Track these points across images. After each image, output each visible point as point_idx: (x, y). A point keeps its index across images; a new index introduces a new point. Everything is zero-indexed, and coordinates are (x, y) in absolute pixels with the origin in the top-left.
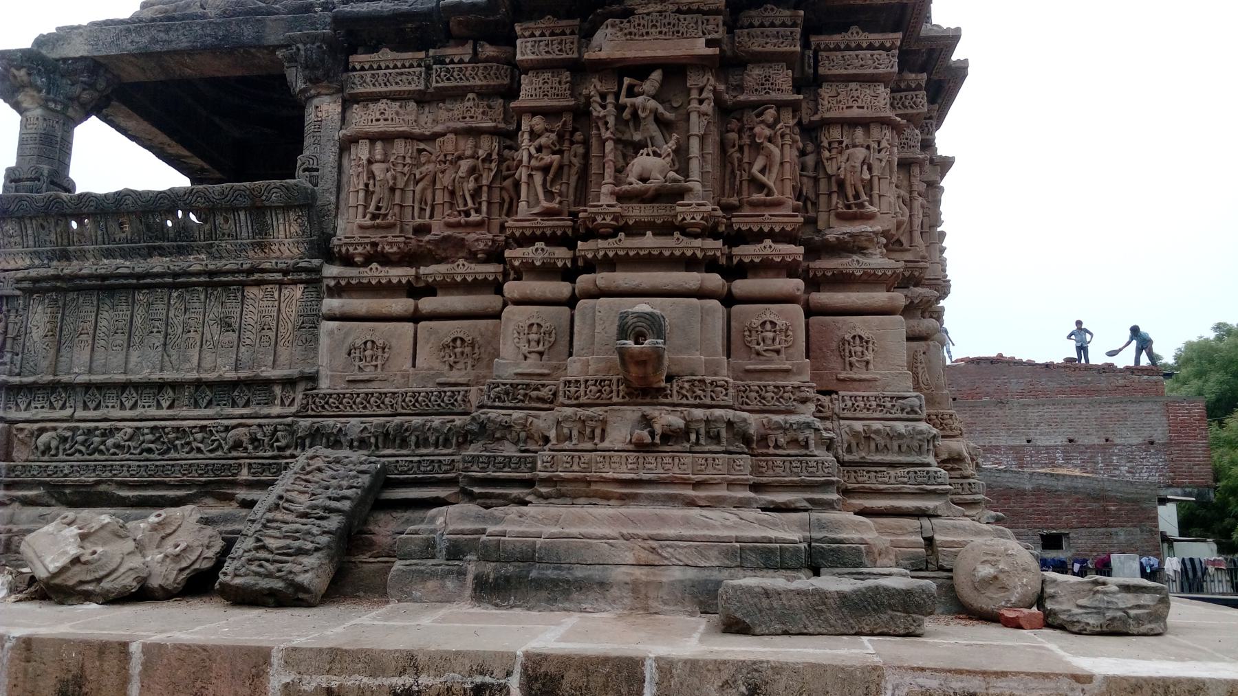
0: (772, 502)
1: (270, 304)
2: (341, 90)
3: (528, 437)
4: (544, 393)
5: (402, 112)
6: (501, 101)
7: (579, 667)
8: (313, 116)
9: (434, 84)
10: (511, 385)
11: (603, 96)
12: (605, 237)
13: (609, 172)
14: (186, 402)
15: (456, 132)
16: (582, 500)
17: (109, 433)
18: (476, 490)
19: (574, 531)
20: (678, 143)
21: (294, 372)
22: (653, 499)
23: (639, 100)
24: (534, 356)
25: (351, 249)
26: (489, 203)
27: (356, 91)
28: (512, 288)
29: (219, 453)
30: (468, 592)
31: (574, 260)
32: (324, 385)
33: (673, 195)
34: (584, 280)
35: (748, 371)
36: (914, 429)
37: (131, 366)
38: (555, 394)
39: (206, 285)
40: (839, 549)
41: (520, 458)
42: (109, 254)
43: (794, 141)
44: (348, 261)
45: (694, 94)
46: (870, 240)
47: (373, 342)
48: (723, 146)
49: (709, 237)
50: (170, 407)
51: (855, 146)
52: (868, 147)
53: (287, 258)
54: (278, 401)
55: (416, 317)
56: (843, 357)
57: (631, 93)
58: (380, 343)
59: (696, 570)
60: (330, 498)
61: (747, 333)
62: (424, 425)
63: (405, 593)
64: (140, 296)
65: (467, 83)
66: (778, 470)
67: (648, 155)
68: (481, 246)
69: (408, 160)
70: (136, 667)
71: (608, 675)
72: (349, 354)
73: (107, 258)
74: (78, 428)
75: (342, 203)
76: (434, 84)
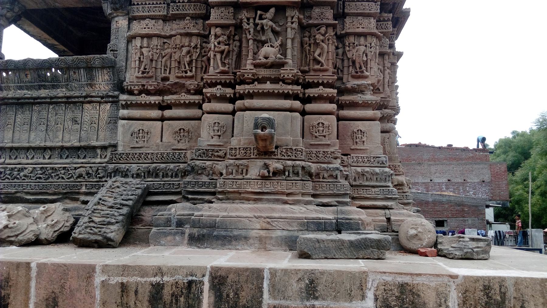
0: (321, 202)
1: (95, 112)
2: (128, 14)
3: (214, 173)
4: (221, 153)
5: (156, 25)
6: (202, 21)
7: (235, 273)
8: (115, 26)
9: (171, 12)
10: (206, 150)
11: (248, 19)
12: (248, 84)
13: (251, 54)
14: (57, 156)
15: (181, 35)
16: (237, 201)
17: (22, 170)
18: (190, 196)
19: (233, 214)
20: (282, 41)
21: (106, 143)
22: (269, 201)
23: (264, 21)
24: (216, 137)
25: (132, 87)
26: (196, 68)
27: (135, 14)
28: (206, 106)
29: (72, 179)
30: (186, 242)
31: (235, 94)
32: (120, 149)
33: (279, 65)
34: (239, 103)
35: (311, 145)
36: (383, 171)
37: (31, 139)
38: (225, 154)
39: (65, 103)
40: (350, 223)
41: (210, 182)
42: (21, 88)
43: (333, 42)
44: (131, 93)
45: (289, 19)
46: (366, 88)
47: (143, 130)
48: (302, 44)
49: (295, 84)
50: (49, 158)
51: (360, 45)
52: (366, 46)
53: (103, 91)
54: (99, 156)
55: (162, 119)
56: (353, 139)
57: (261, 18)
58: (146, 130)
59: (287, 232)
60: (123, 200)
61: (311, 128)
62: (166, 168)
63: (157, 242)
64: (35, 108)
65: (186, 12)
66: (324, 188)
67: (268, 46)
68: (192, 87)
69: (159, 47)
70: (34, 274)
71: (248, 276)
72: (132, 135)
73: (20, 90)
74: (7, 168)
75: (128, 66)
76: (171, 12)
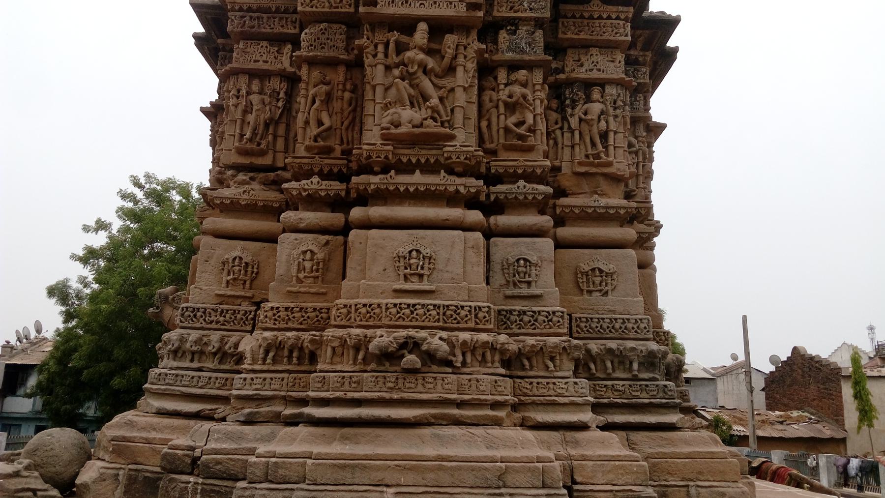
31: (348, 191)
34: (356, 213)
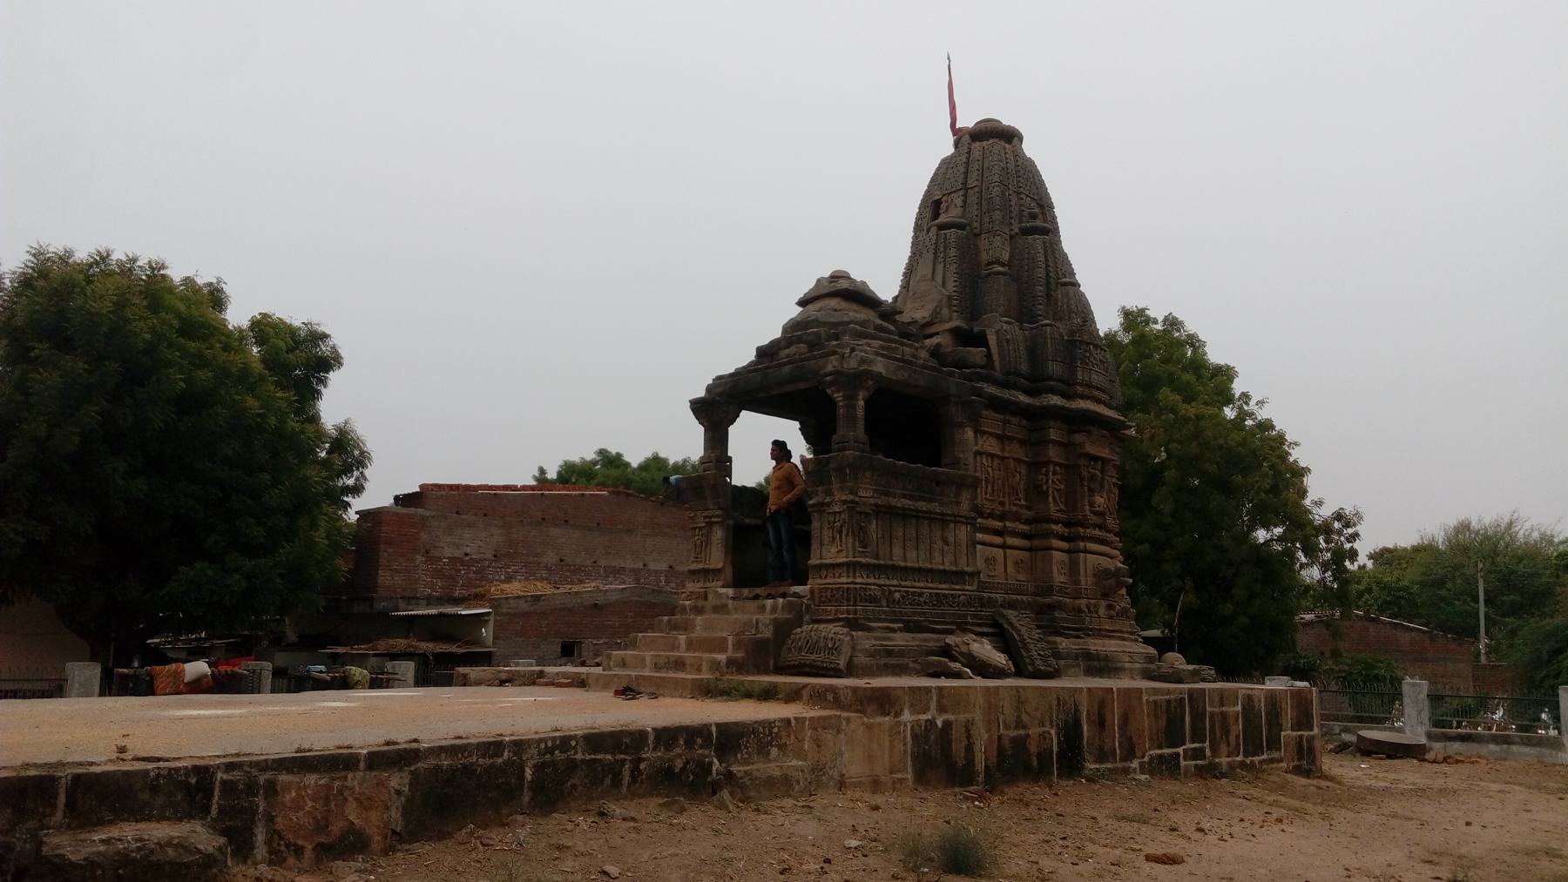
42: (904, 496)
55: (1003, 546)
